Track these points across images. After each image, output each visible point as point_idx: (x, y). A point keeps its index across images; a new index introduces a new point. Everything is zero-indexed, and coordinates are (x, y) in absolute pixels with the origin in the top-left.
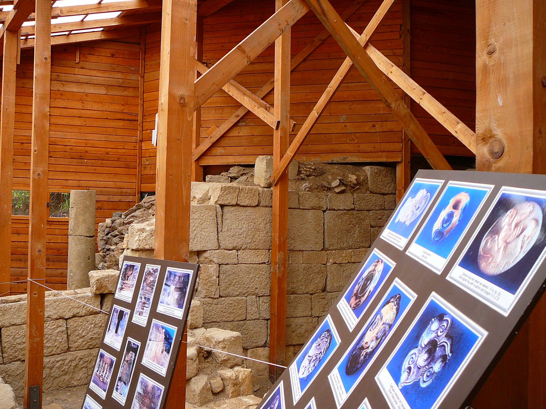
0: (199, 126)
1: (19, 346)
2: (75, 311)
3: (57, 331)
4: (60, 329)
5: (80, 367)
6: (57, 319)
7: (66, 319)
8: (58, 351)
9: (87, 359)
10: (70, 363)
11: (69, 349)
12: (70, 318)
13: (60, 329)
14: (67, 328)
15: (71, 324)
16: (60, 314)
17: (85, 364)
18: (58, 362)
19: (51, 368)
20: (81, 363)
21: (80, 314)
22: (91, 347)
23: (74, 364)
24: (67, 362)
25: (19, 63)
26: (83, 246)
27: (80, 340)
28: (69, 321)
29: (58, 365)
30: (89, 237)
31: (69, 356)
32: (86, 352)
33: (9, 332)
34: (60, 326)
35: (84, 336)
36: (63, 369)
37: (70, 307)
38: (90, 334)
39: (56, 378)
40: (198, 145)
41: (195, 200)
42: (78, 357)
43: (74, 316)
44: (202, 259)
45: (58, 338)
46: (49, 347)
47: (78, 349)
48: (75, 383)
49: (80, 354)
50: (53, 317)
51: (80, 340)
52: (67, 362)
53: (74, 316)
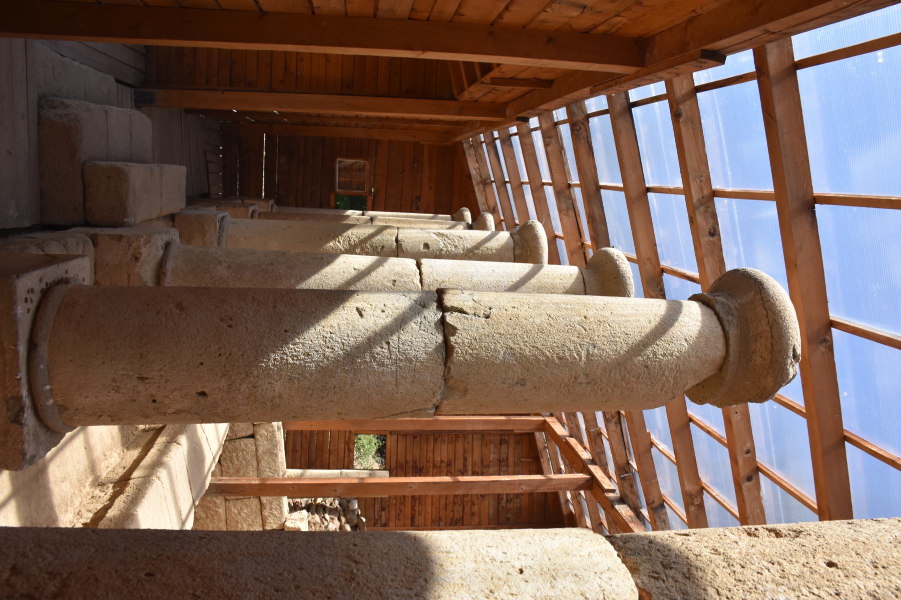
1: (234, 454)
23: (211, 505)
27: (236, 511)
32: (223, 517)
33: (249, 445)
47: (227, 509)
49: (221, 511)
51: (236, 511)
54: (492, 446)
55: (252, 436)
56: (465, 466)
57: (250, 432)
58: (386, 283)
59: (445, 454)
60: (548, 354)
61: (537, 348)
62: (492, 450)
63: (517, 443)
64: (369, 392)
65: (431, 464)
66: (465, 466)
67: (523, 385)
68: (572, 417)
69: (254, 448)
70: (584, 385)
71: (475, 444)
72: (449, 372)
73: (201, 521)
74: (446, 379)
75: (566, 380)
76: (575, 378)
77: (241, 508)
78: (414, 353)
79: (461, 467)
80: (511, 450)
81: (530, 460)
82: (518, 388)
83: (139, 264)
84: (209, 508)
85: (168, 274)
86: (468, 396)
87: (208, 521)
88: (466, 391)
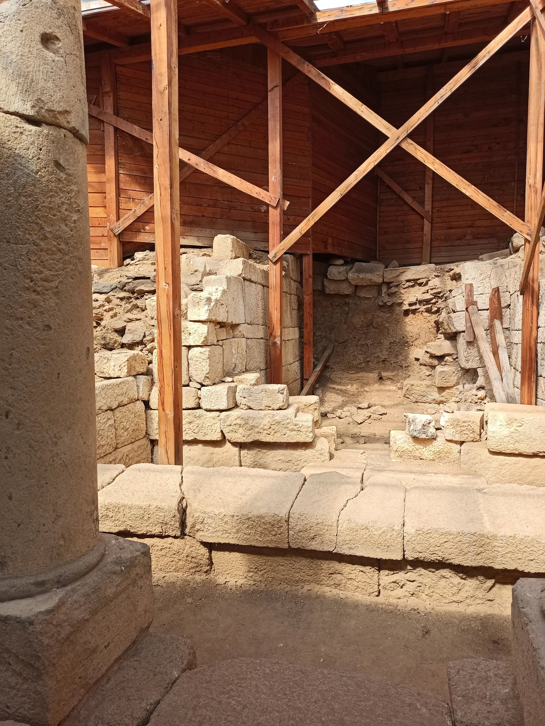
0: (118, 195)
2: (120, 399)
3: (108, 425)
6: (107, 410)
12: (116, 408)
14: (115, 420)
21: (124, 402)
22: (133, 441)
27: (126, 433)
28: (116, 411)
34: (109, 419)
37: (115, 395)
40: (118, 219)
41: (196, 273)
42: (125, 455)
44: (237, 333)
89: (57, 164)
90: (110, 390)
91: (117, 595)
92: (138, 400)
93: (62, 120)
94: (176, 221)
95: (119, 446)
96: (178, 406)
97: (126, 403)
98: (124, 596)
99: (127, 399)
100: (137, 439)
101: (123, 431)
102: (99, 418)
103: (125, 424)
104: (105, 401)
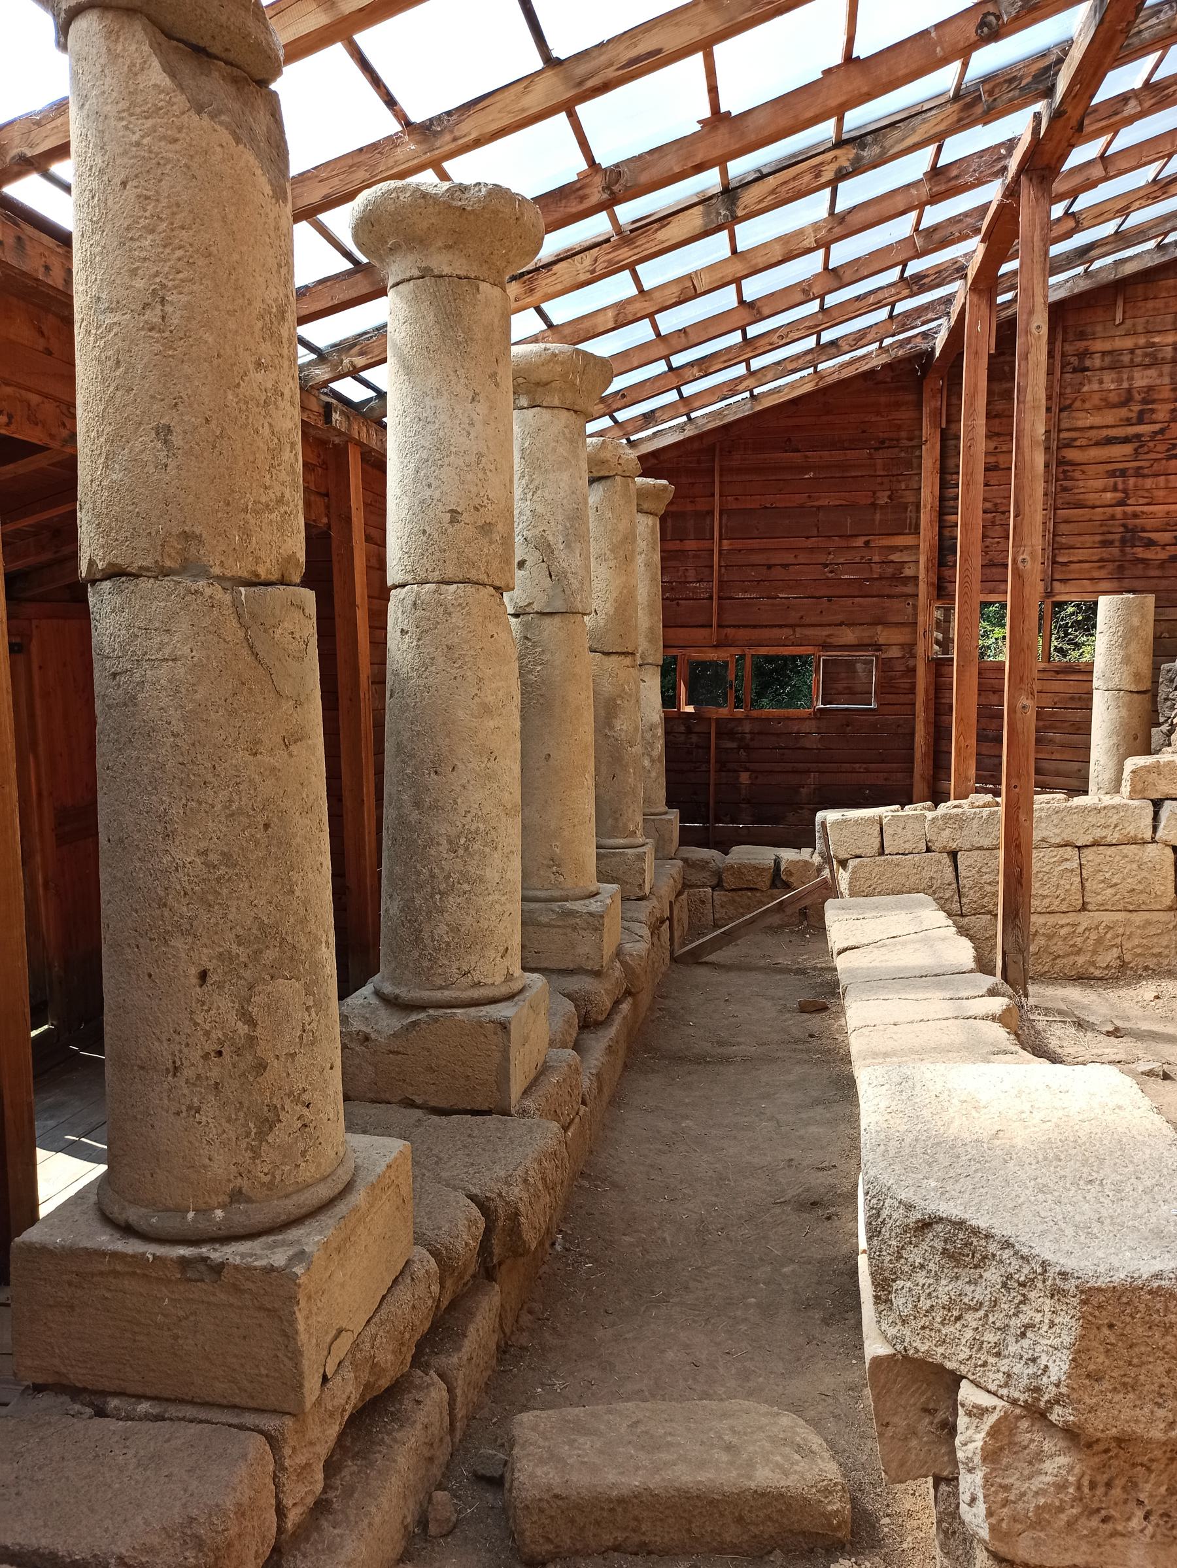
2: (1098, 833)
4: (1067, 865)
5: (1107, 943)
7: (1079, 848)
8: (1064, 908)
9: (1121, 931)
10: (1087, 933)
11: (1084, 908)
12: (1086, 846)
13: (1067, 865)
15: (1090, 859)
16: (1067, 836)
17: (1118, 941)
18: (1062, 926)
19: (1050, 937)
20: (1109, 936)
22: (1131, 908)
23: (1094, 936)
24: (1080, 929)
25: (993, 352)
26: (1124, 713)
27: (1110, 891)
28: (1085, 851)
29: (1063, 932)
30: (1138, 692)
31: (1085, 920)
32: (1120, 916)
34: (1067, 860)
35: (1116, 885)
36: (1071, 943)
37: (1086, 825)
38: (1129, 880)
39: (1059, 956)
43: (1096, 844)
45: (1062, 882)
46: (1045, 897)
47: (1102, 908)
48: (1097, 973)
49: (1107, 918)
50: (1053, 841)
52: (1080, 929)
53: (1096, 844)
54: (1085, 389)
55: (953, 855)
56: (1126, 440)
57: (946, 859)
58: (405, 646)
59: (1099, 484)
60: (111, 389)
61: (104, 410)
62: (1096, 387)
63: (1082, 336)
64: (190, 706)
65: (1119, 509)
66: (1126, 440)
67: (168, 429)
68: (937, 237)
69: (976, 853)
70: (169, 309)
71: (1080, 424)
72: (148, 569)
73: (1127, 958)
74: (166, 573)
75: (158, 347)
76: (151, 330)
77: (1103, 881)
78: (123, 632)
79: (1128, 449)
80: (1099, 346)
81: (1120, 303)
82: (176, 439)
83: (373, 1036)
84: (1099, 941)
85: (397, 991)
86: (197, 530)
87: (1128, 945)
88: (186, 536)
89: (526, 638)
90: (1075, 816)
91: (548, 925)
92: (1153, 841)
93: (528, 610)
94: (1029, 565)
95: (1089, 907)
96: (1018, 846)
97: (1114, 842)
98: (560, 931)
99: (1116, 835)
100: (1143, 907)
101: (1102, 885)
102: (1041, 855)
103: (1107, 875)
104: (1057, 831)
